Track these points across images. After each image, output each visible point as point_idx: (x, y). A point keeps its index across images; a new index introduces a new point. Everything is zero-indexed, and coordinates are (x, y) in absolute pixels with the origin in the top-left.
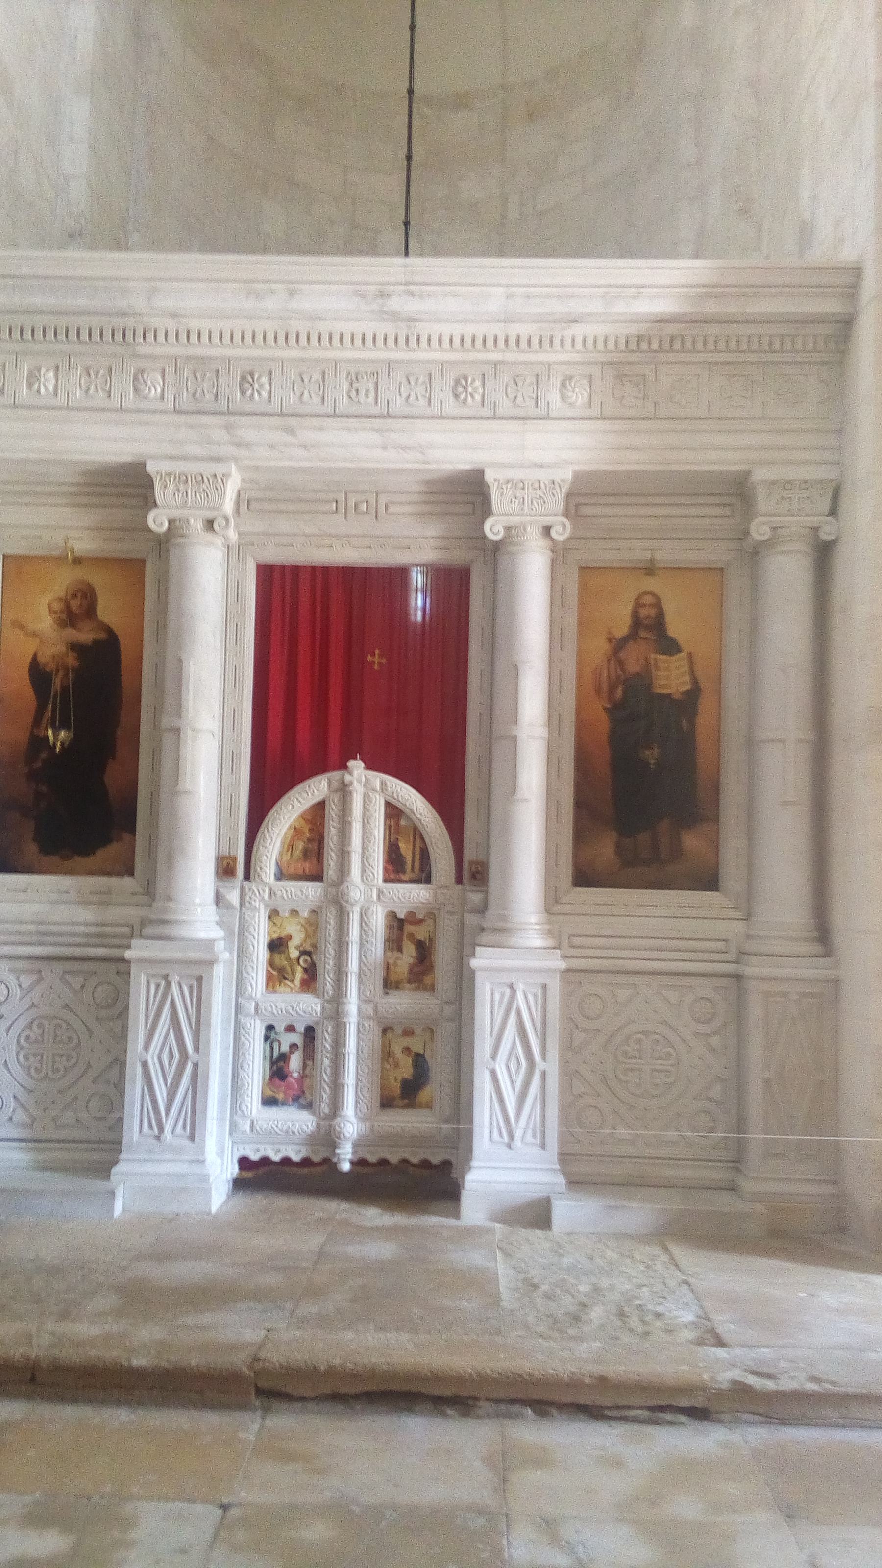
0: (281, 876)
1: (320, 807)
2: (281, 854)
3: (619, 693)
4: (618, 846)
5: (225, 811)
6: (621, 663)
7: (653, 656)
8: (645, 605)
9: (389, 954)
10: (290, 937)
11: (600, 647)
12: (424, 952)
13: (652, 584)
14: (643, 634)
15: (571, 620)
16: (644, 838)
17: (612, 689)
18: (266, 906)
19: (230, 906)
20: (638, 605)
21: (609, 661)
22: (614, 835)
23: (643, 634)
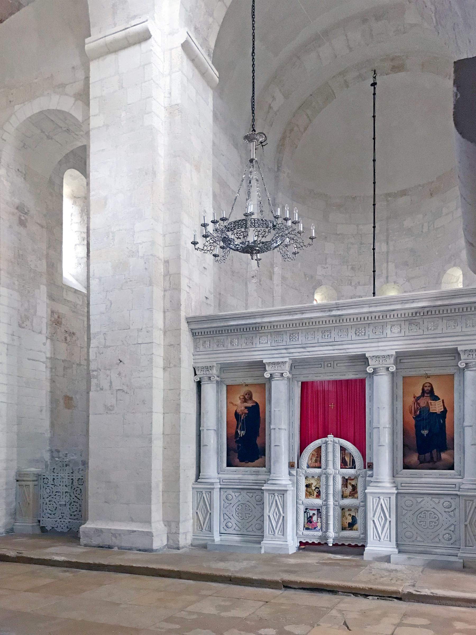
0: (308, 467)
1: (320, 447)
2: (308, 461)
3: (418, 413)
4: (419, 457)
5: (290, 449)
6: (418, 404)
7: (430, 401)
8: (426, 386)
9: (343, 488)
10: (312, 484)
11: (411, 400)
12: (354, 488)
13: (429, 380)
14: (426, 395)
15: (400, 392)
16: (428, 455)
17: (415, 412)
18: (304, 475)
19: (293, 475)
20: (424, 386)
21: (414, 404)
22: (417, 454)
23: (426, 395)
